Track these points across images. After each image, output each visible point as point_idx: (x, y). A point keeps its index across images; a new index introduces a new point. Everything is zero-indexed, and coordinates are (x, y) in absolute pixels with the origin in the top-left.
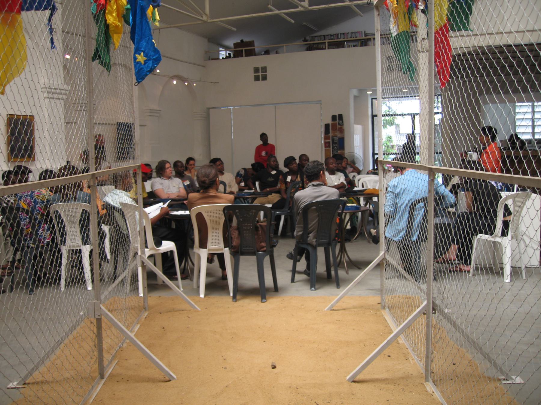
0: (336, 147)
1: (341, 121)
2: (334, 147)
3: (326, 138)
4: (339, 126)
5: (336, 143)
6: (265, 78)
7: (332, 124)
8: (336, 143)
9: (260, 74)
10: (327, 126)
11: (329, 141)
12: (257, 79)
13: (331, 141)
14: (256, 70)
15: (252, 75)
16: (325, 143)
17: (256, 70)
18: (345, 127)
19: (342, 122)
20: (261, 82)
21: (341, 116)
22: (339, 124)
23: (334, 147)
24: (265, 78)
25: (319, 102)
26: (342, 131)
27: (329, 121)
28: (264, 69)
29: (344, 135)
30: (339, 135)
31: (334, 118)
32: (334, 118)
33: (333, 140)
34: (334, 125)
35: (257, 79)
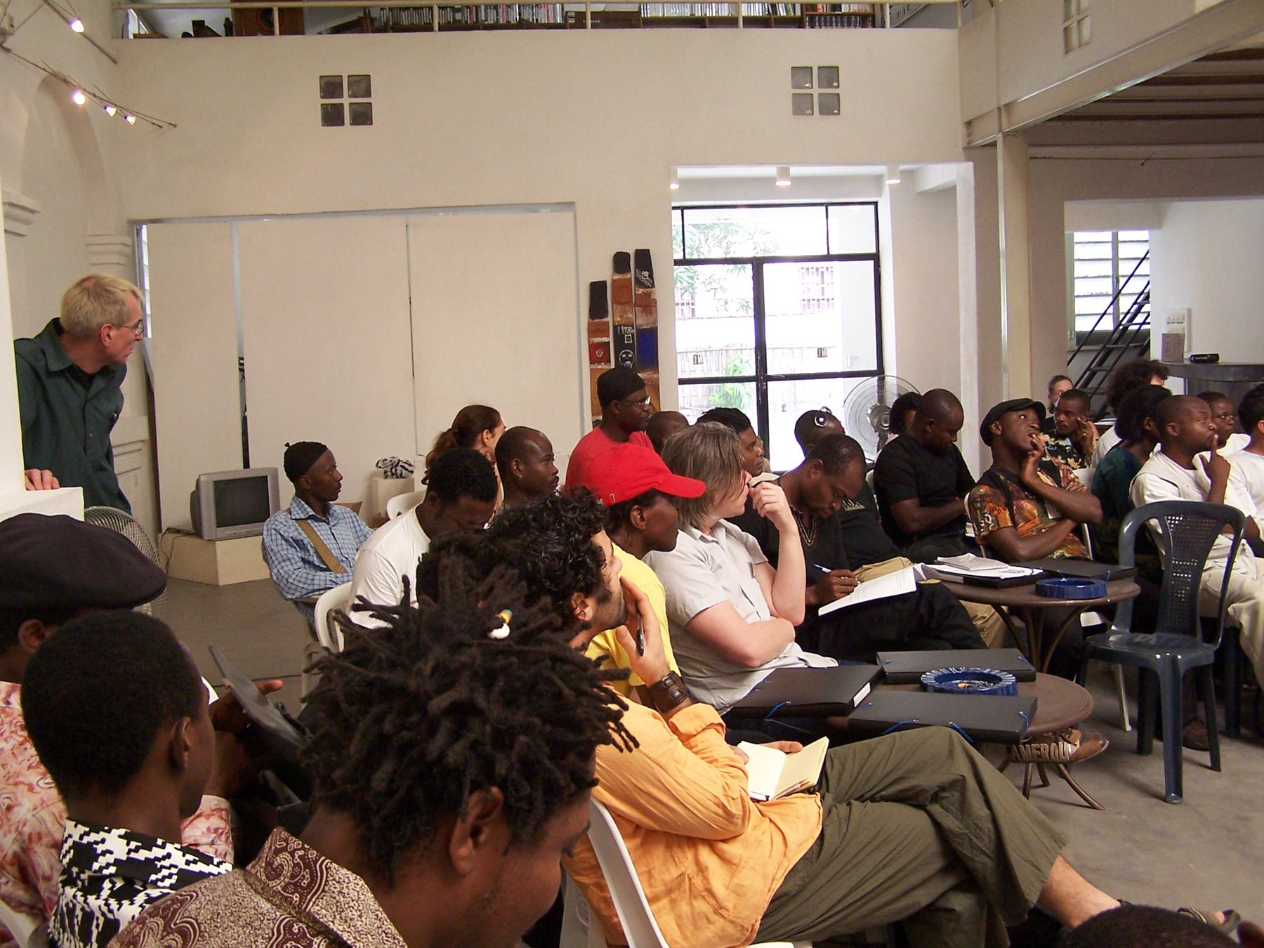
0: (631, 359)
1: (646, 273)
2: (624, 360)
3: (593, 331)
4: (640, 291)
5: (631, 347)
6: (363, 116)
7: (614, 281)
8: (631, 347)
9: (346, 101)
10: (597, 290)
11: (605, 339)
12: (332, 117)
13: (610, 339)
14: (331, 87)
15: (315, 102)
16: (593, 348)
17: (331, 87)
18: (659, 293)
19: (651, 276)
20: (348, 132)
21: (644, 258)
22: (639, 283)
23: (624, 360)
24: (363, 116)
25: (570, 205)
26: (648, 305)
27: (605, 272)
28: (362, 85)
29: (655, 321)
30: (642, 321)
31: (620, 261)
32: (620, 261)
33: (619, 338)
34: (619, 287)
35: (332, 117)
